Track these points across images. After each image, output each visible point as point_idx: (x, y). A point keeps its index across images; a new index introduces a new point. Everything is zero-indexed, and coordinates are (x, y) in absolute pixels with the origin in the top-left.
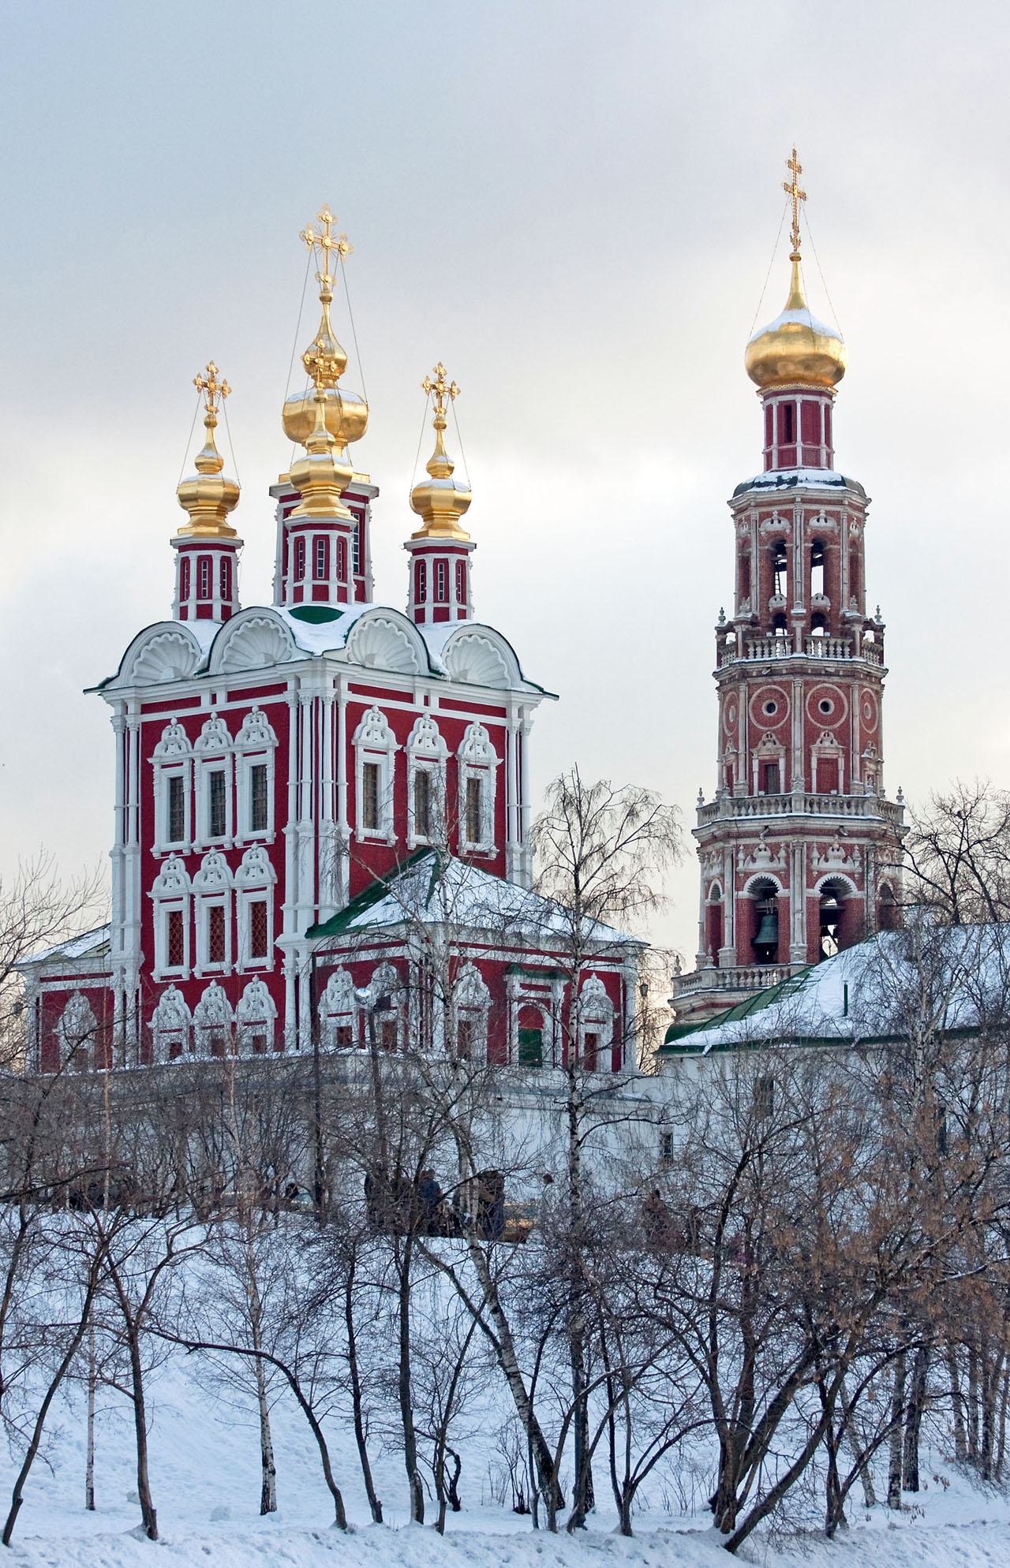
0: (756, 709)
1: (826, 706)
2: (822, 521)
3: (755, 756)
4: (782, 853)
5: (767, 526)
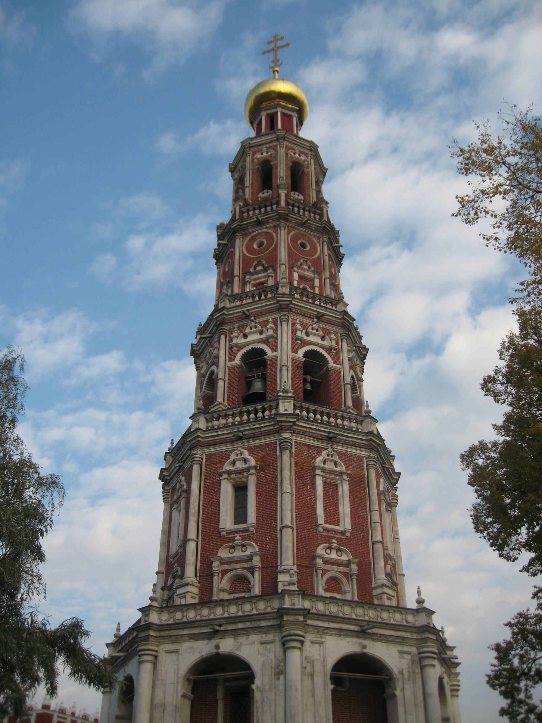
0: (250, 249)
1: (303, 245)
2: (297, 155)
4: (270, 325)
5: (259, 156)
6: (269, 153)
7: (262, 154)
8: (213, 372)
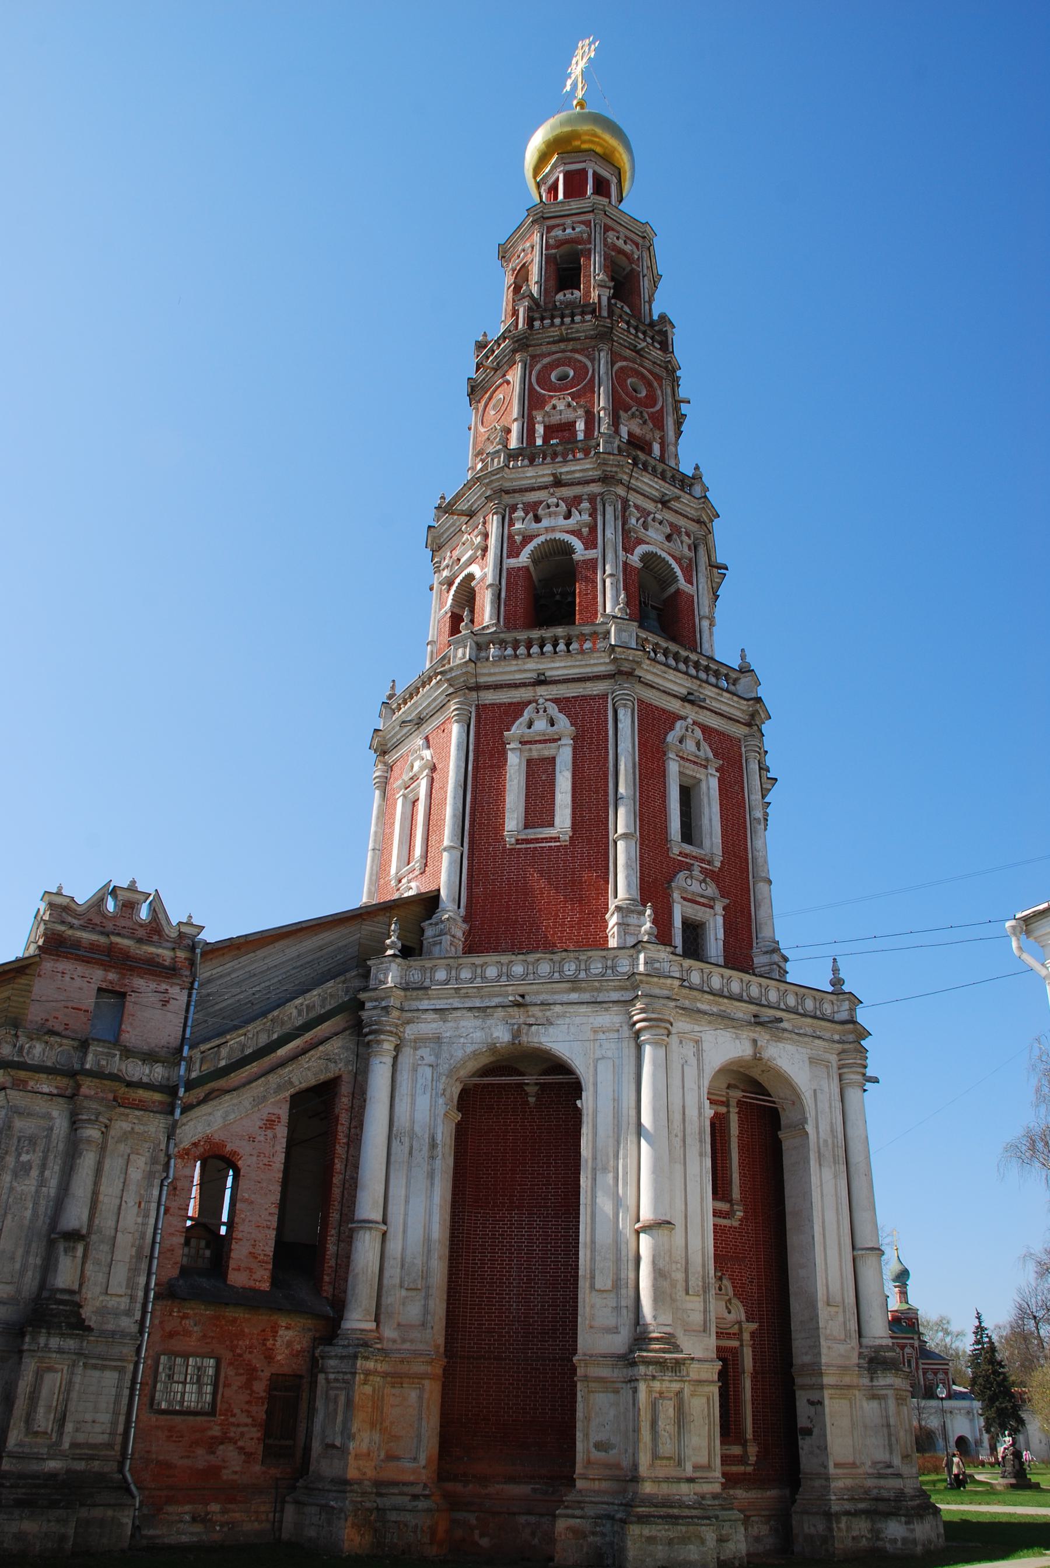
3: (539, 418)
4: (586, 505)
5: (558, 233)
6: (578, 230)
7: (564, 230)
8: (470, 577)
